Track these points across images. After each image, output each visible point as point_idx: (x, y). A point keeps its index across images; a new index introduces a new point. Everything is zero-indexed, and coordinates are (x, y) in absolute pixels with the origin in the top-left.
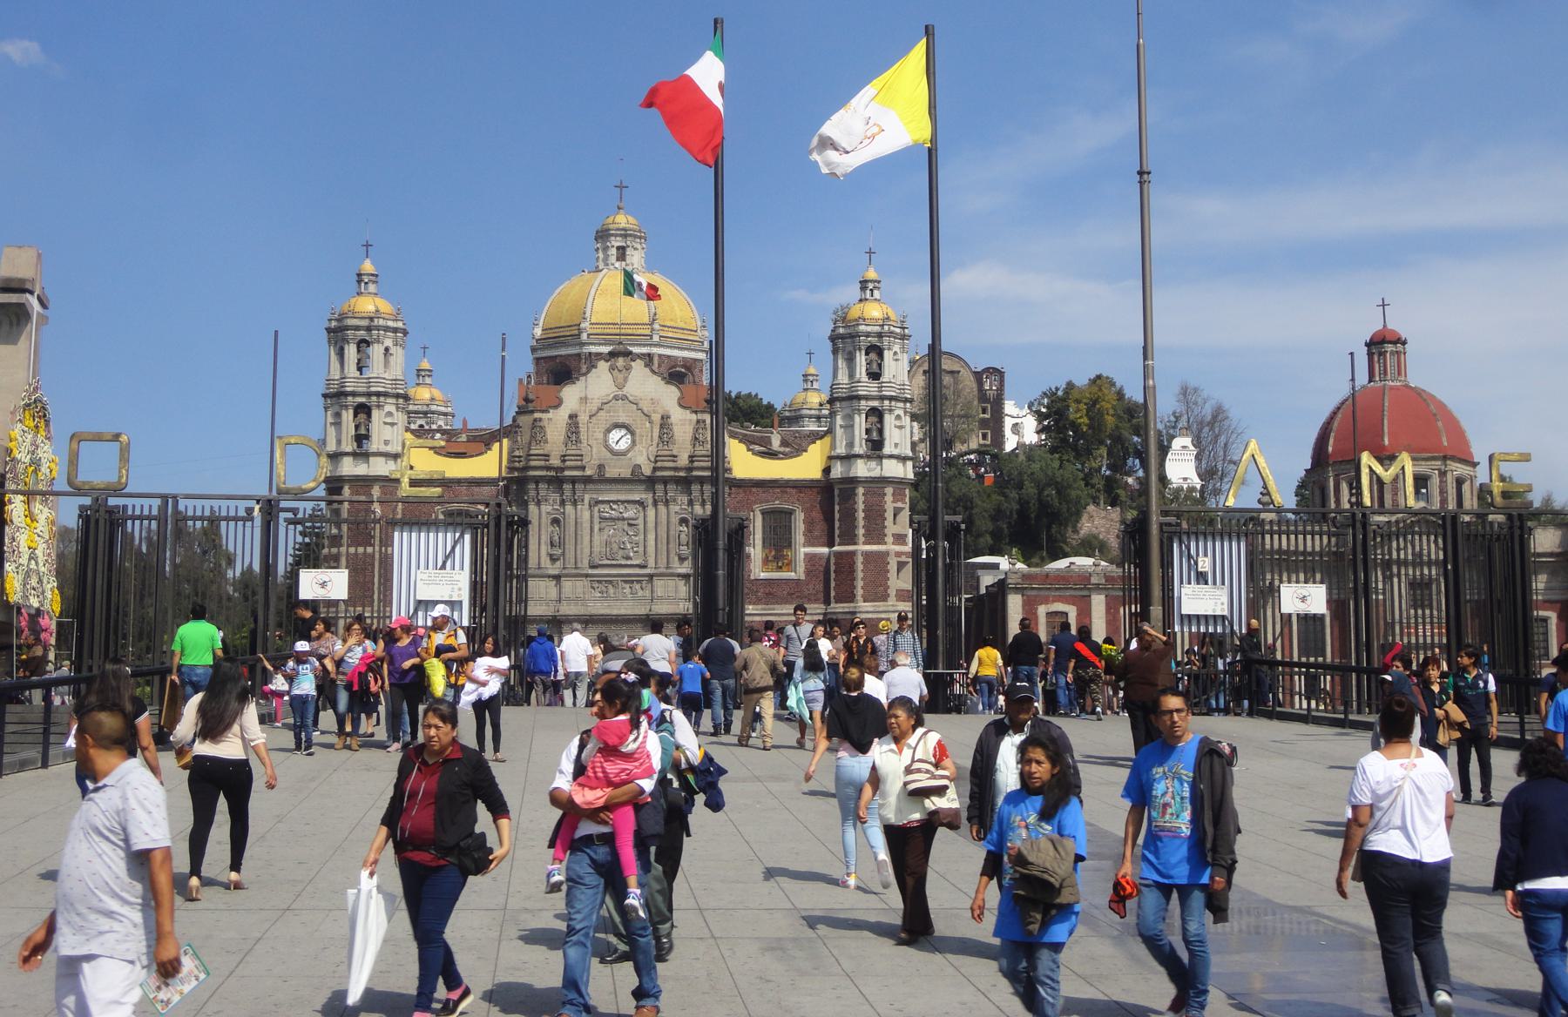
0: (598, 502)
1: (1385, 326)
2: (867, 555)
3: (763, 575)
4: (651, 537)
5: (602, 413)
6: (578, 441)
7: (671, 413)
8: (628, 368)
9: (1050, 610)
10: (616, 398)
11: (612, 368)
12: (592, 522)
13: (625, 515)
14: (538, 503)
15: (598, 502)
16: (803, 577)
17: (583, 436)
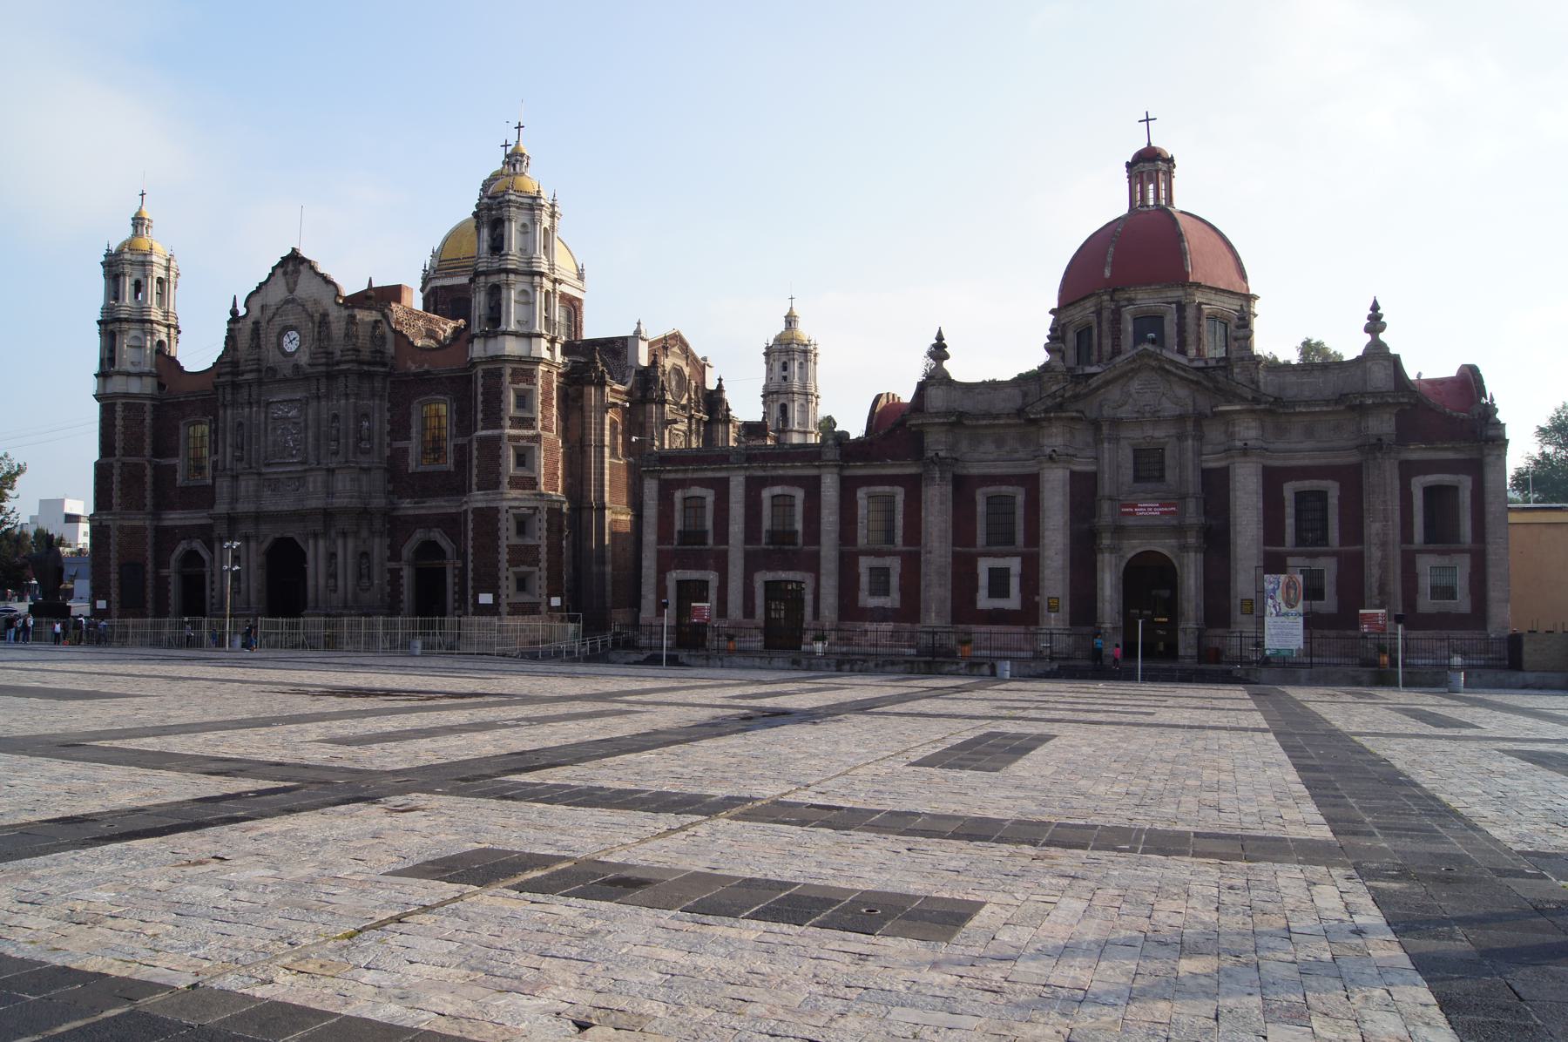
0: (269, 404)
1: (1149, 144)
2: (482, 440)
3: (419, 470)
4: (310, 434)
5: (277, 318)
6: (259, 346)
7: (330, 311)
8: (297, 272)
9: (687, 495)
10: (287, 302)
11: (285, 273)
12: (266, 423)
13: (289, 415)
14: (225, 406)
15: (269, 404)
16: (452, 469)
17: (263, 343)
